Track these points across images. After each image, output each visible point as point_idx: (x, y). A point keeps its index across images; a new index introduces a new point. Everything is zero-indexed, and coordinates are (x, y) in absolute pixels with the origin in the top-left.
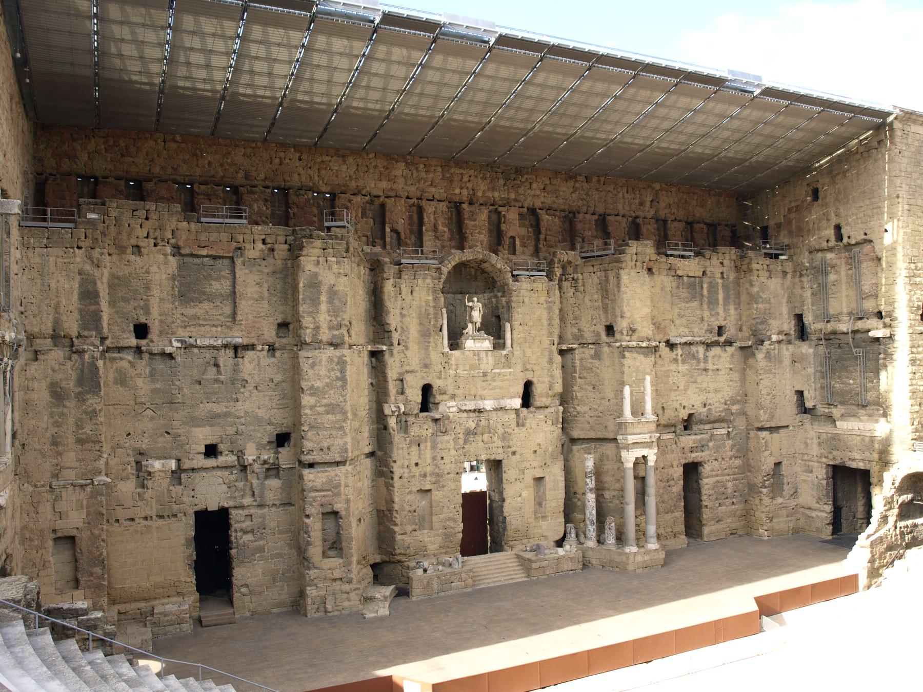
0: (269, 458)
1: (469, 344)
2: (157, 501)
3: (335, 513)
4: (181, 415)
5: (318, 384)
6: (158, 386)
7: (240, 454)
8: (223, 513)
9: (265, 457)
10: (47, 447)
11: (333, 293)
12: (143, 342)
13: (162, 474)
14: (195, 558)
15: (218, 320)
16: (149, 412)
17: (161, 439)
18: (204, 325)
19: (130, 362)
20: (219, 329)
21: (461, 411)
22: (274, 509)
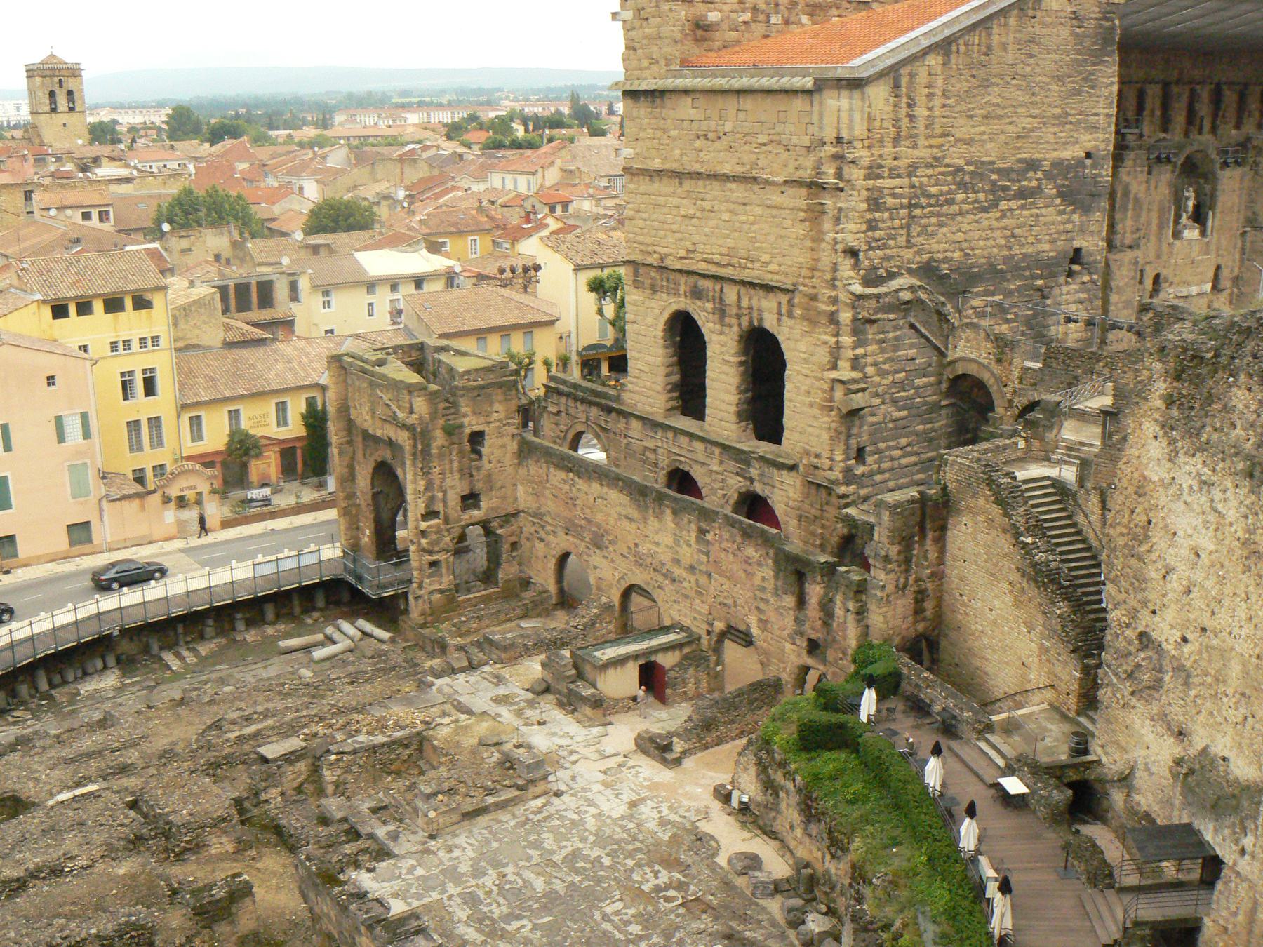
1: (1186, 234)
11: (1137, 200)
21: (1177, 297)
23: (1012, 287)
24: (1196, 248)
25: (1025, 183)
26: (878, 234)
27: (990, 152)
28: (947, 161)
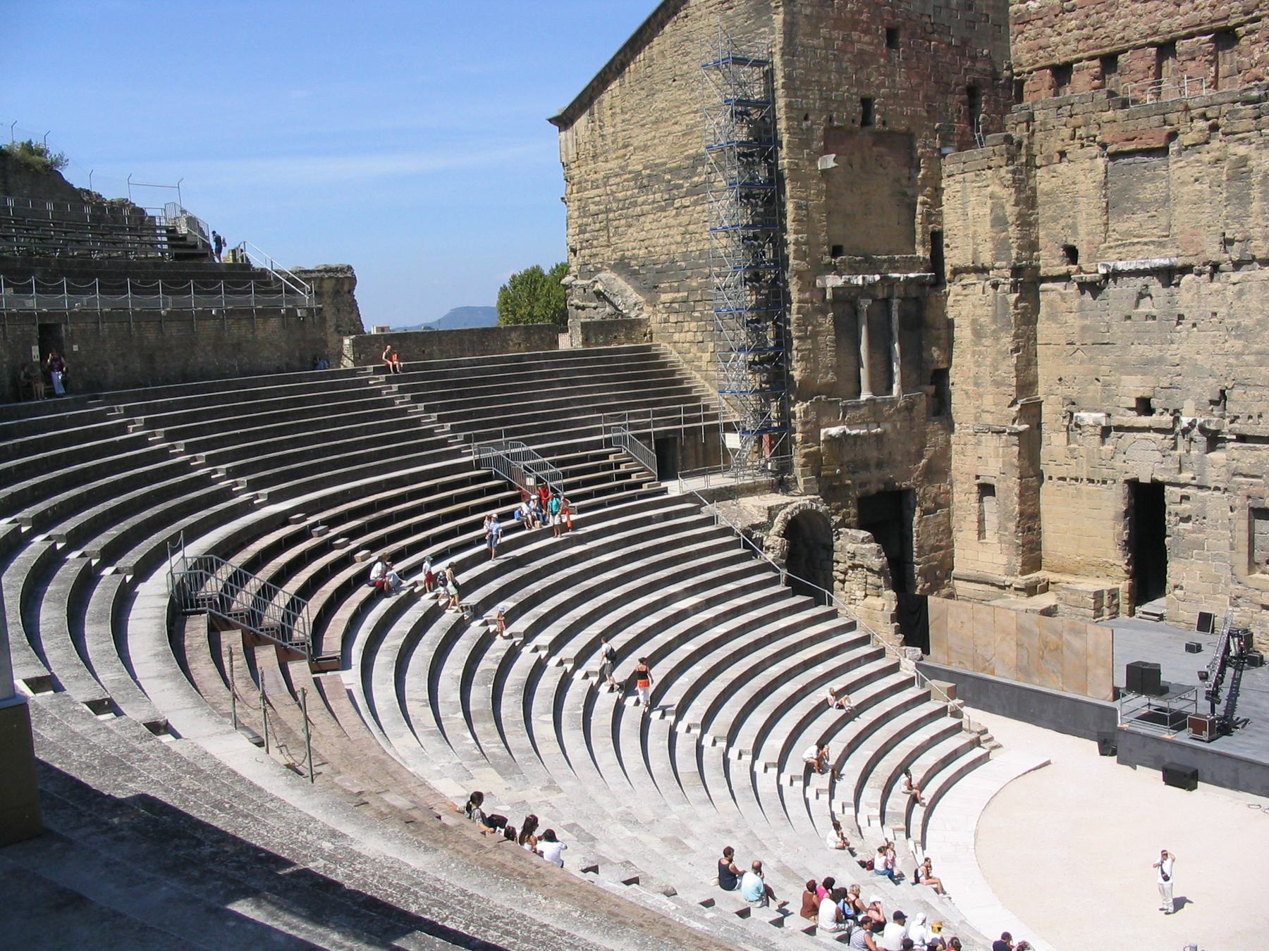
0: (1209, 422)
2: (1088, 461)
4: (1107, 359)
5: (1246, 322)
6: (1088, 322)
7: (1176, 414)
8: (1156, 489)
9: (1200, 421)
10: (971, 388)
12: (1073, 268)
13: (1092, 430)
14: (1125, 538)
15: (1153, 234)
16: (1079, 353)
17: (1091, 387)
18: (1134, 244)
19: (1060, 294)
20: (1152, 247)
22: (1217, 493)
23: (694, 284)
25: (696, 179)
26: (587, 235)
27: (660, 154)
28: (630, 168)
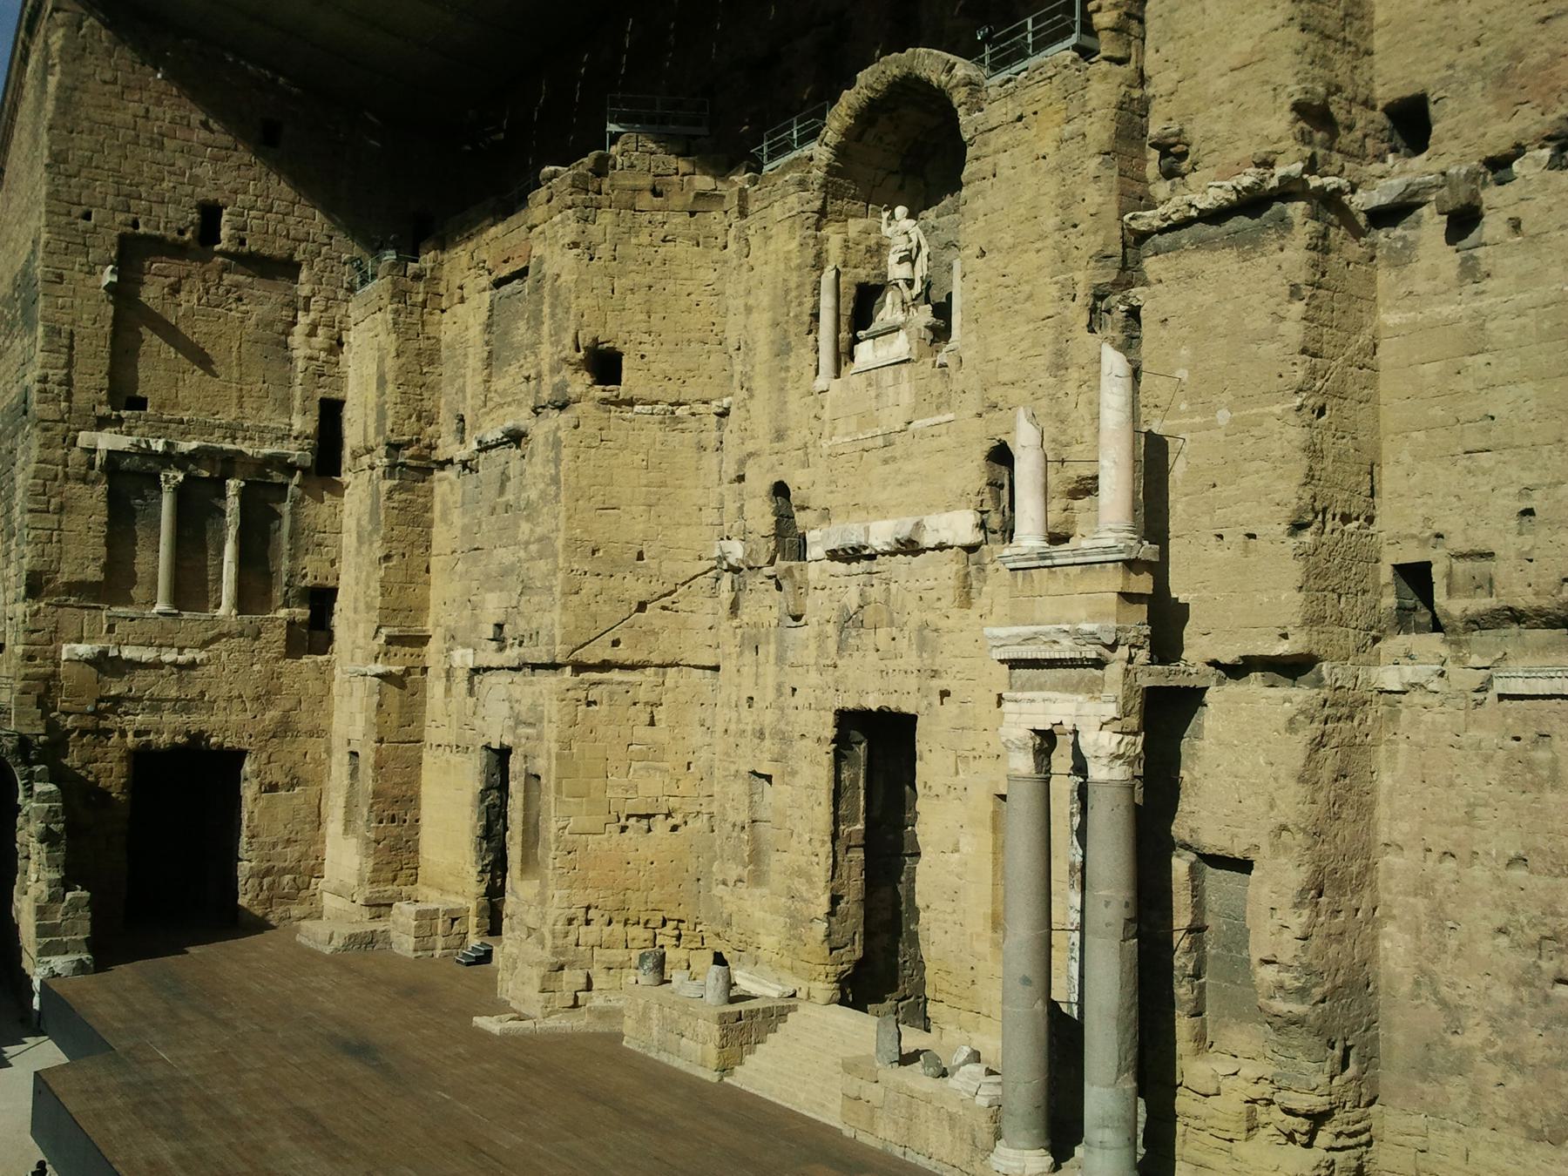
3: (538, 777)
24: (903, 392)
